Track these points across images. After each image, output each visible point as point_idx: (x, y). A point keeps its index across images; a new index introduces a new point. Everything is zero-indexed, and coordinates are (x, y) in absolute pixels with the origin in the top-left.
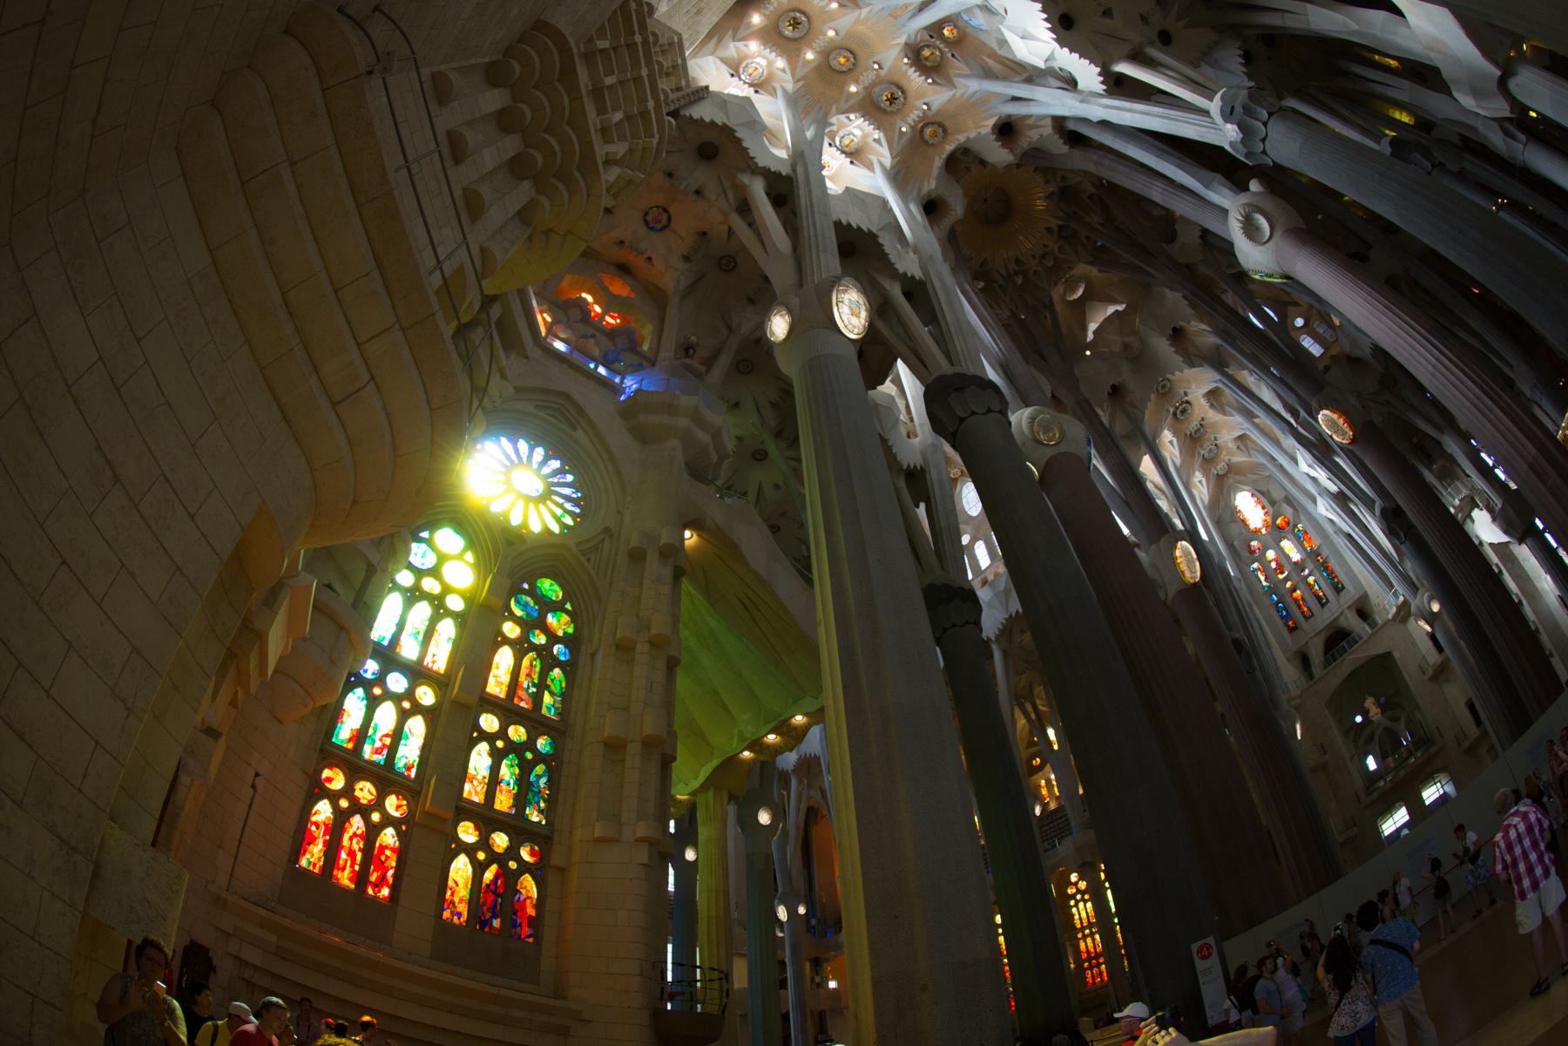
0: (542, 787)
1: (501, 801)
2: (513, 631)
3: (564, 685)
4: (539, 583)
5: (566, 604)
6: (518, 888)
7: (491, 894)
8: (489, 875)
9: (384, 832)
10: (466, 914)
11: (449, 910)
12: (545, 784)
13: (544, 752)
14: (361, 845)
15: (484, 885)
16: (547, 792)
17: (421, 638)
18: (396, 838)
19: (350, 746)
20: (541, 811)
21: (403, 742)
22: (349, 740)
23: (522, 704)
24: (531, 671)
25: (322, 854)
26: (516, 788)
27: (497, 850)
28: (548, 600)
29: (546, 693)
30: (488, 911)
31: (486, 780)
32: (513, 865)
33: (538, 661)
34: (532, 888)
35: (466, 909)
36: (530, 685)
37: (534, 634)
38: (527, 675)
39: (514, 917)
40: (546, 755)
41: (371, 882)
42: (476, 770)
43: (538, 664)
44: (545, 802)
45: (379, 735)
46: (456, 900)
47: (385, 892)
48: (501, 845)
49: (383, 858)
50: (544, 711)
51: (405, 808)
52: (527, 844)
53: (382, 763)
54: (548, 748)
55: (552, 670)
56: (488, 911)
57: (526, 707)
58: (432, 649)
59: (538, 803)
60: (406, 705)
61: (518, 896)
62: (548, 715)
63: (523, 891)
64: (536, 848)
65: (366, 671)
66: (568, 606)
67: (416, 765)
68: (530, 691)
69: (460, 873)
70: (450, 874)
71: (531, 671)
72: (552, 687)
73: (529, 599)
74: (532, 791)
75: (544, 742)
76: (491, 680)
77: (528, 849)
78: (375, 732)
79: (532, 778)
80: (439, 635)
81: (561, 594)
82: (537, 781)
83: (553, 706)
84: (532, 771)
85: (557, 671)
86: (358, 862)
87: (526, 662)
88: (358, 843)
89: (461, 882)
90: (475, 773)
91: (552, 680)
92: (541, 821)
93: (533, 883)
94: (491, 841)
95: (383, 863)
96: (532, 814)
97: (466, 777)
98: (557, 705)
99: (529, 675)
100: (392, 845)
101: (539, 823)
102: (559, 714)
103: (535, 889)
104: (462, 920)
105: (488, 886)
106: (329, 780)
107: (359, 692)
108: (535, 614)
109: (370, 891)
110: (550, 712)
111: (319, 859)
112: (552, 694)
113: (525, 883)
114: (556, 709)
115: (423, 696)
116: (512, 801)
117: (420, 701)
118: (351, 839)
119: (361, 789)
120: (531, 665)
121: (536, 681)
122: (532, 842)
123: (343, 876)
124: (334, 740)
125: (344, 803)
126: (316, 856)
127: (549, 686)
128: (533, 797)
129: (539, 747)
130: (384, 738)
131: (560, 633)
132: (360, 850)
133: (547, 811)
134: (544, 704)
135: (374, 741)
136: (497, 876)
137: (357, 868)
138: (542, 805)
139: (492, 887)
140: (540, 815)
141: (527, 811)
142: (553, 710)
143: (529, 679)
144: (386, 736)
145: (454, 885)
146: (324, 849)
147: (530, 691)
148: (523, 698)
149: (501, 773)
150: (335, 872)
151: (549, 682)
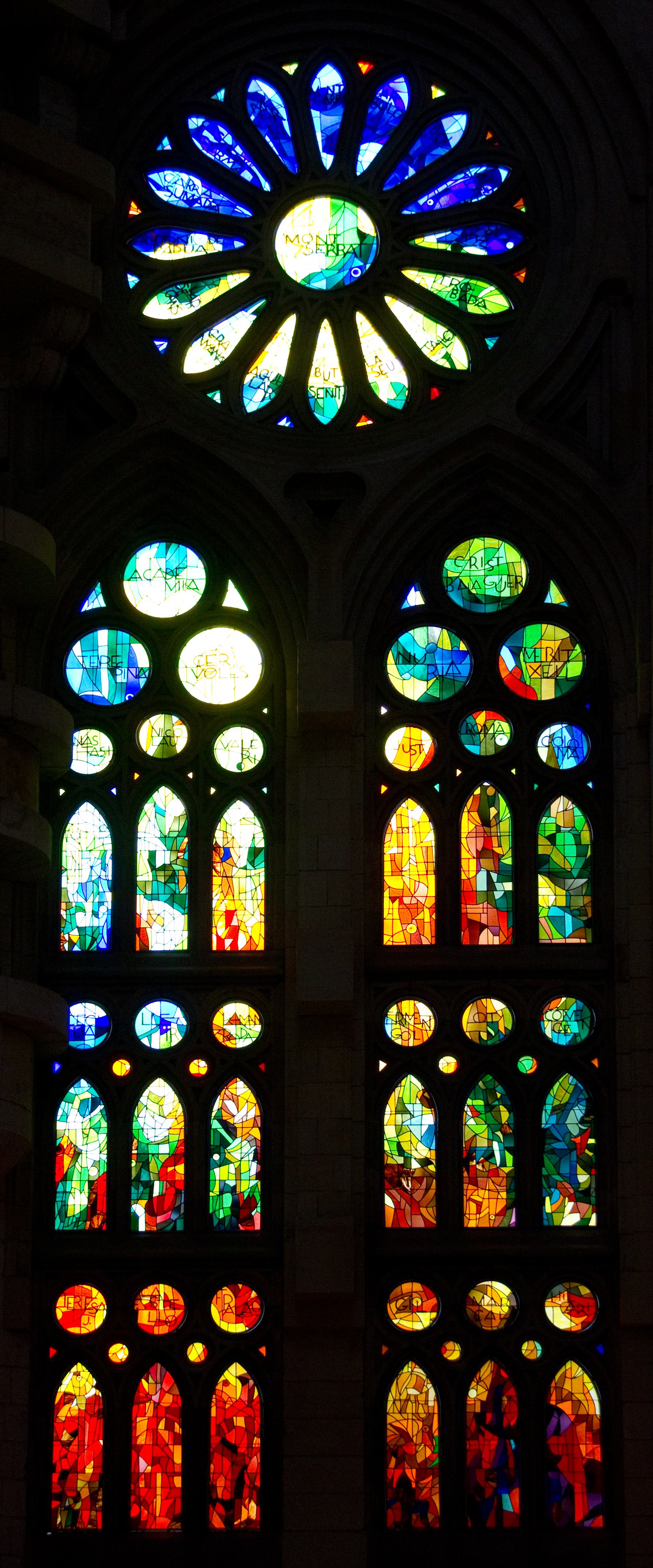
0: (574, 1130)
1: (479, 1205)
2: (411, 749)
3: (586, 838)
4: (451, 567)
5: (547, 590)
6: (553, 1403)
7: (489, 1435)
8: (476, 1393)
9: (222, 1378)
10: (436, 1499)
11: (398, 1505)
12: (582, 1121)
13: (563, 1041)
14: (177, 1428)
15: (470, 1417)
16: (591, 1141)
17: (183, 888)
18: (251, 1382)
19: (97, 1222)
20: (580, 1196)
21: (216, 1157)
22: (91, 1210)
23: (486, 938)
24: (488, 840)
25: (97, 1484)
26: (509, 1158)
27: (486, 1326)
28: (490, 608)
29: (542, 881)
30: (487, 1479)
31: (432, 1168)
32: (531, 1349)
33: (503, 803)
34: (586, 1393)
35: (436, 1489)
36: (494, 876)
37: (472, 732)
38: (479, 855)
39: (550, 1474)
40: (572, 1048)
41: (218, 1500)
42: (401, 1151)
43: (503, 809)
44: (587, 1168)
45: (155, 1166)
46: (411, 1474)
47: (251, 1510)
48: (496, 1310)
49: (232, 1438)
50: (548, 933)
51: (256, 1305)
52: (556, 1289)
53: (180, 1226)
54: (574, 1027)
55: (543, 808)
56: (487, 1479)
57: (496, 941)
58: (219, 904)
59: (572, 1177)
60: (199, 1067)
61: (554, 1421)
62: (558, 939)
63: (566, 1407)
64: (585, 1291)
65: (80, 1032)
66: (555, 596)
67: (258, 1198)
68: (498, 895)
69: (410, 1408)
70: (390, 1419)
71: (488, 840)
72: (556, 858)
73: (436, 632)
74: (553, 1151)
75: (557, 1015)
76: (390, 910)
77: (563, 1300)
78: (145, 1164)
79: (547, 1119)
80: (227, 855)
81: (522, 570)
82: (561, 1123)
83: (567, 908)
84: (543, 1103)
85: (560, 805)
86: (178, 1469)
87: (468, 823)
88: (169, 1427)
89: (414, 1429)
90: (401, 1160)
91: (552, 838)
92: (585, 1220)
93: (587, 1379)
94: (470, 1310)
95: (233, 1448)
96: (561, 1210)
97: (383, 1177)
98: (579, 902)
99: (484, 853)
100: (245, 1398)
101: (582, 1228)
102: (588, 924)
103: (594, 1394)
104: (431, 1517)
105: (479, 1418)
106: (74, 1316)
107: (83, 1090)
108: (465, 668)
109: (217, 1522)
110: (561, 929)
111: (93, 1496)
112: (557, 877)
113: (567, 1386)
114: (577, 913)
115: (232, 1029)
116: (504, 1195)
117: (228, 1044)
118: (152, 1429)
119: (151, 1306)
120: (486, 822)
121: (508, 861)
122: (570, 1280)
123: (152, 1514)
124: (58, 1225)
125: (119, 1353)
126: (85, 1493)
127: (547, 859)
128: (557, 1166)
129: (548, 1032)
130: (170, 1169)
131: (547, 691)
132: (176, 1440)
133: (597, 1189)
134: (543, 913)
135: (149, 1185)
136: (495, 1391)
137: (178, 1481)
138: (583, 1178)
139: (489, 1417)
140: (584, 1206)
141: (548, 1208)
142: (569, 918)
143: (487, 863)
144: (173, 1159)
145: (402, 1442)
146: (100, 1471)
147: (498, 895)
148: (484, 921)
149: (467, 1135)
150: (134, 1512)
151: (543, 848)
